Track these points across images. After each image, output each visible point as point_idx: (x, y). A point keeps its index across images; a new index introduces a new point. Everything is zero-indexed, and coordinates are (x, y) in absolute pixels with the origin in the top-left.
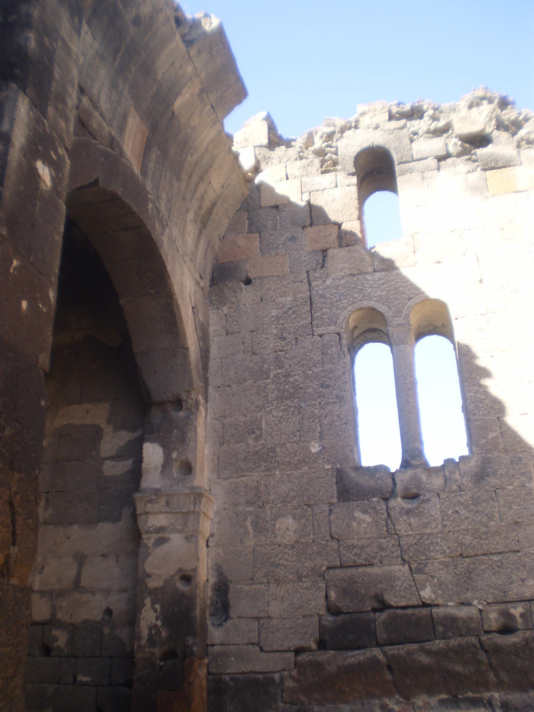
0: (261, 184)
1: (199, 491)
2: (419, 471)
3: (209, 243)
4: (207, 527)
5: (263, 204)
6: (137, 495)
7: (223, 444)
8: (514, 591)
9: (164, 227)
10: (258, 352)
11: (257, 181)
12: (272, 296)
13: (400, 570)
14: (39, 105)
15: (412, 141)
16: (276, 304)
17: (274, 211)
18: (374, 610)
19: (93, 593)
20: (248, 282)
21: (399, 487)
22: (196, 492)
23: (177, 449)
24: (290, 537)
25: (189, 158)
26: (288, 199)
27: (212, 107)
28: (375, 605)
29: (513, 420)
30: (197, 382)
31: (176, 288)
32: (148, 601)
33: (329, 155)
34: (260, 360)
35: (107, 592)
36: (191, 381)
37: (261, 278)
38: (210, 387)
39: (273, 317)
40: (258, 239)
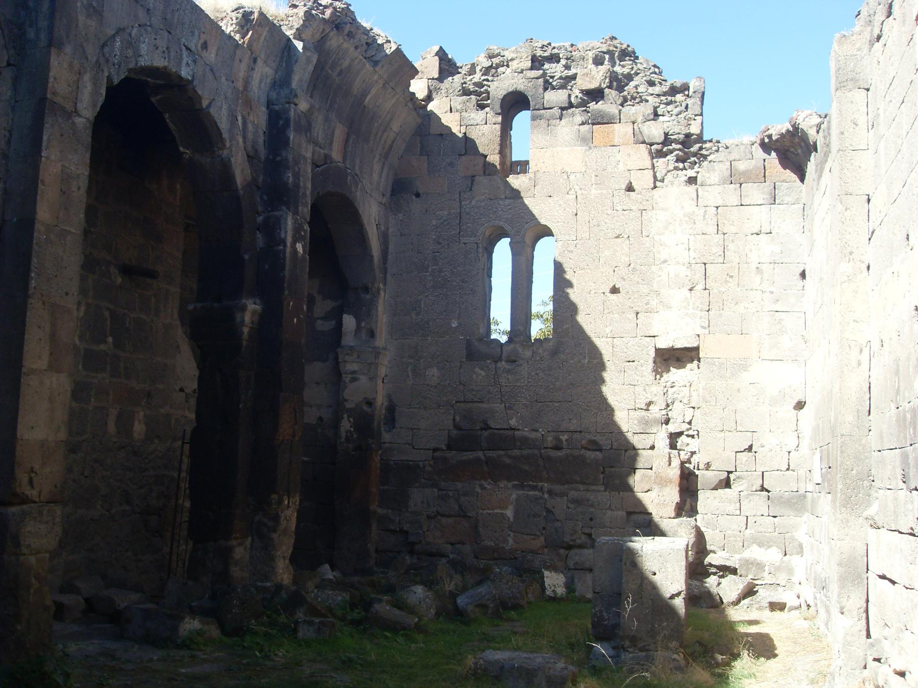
0: (432, 112)
2: (517, 345)
4: (383, 371)
5: (432, 132)
6: (339, 350)
14: (296, 213)
15: (545, 89)
18: (482, 429)
19: (311, 406)
20: (418, 195)
25: (376, 124)
26: (449, 129)
29: (581, 318)
30: (379, 274)
31: (365, 221)
32: (345, 416)
33: (485, 87)
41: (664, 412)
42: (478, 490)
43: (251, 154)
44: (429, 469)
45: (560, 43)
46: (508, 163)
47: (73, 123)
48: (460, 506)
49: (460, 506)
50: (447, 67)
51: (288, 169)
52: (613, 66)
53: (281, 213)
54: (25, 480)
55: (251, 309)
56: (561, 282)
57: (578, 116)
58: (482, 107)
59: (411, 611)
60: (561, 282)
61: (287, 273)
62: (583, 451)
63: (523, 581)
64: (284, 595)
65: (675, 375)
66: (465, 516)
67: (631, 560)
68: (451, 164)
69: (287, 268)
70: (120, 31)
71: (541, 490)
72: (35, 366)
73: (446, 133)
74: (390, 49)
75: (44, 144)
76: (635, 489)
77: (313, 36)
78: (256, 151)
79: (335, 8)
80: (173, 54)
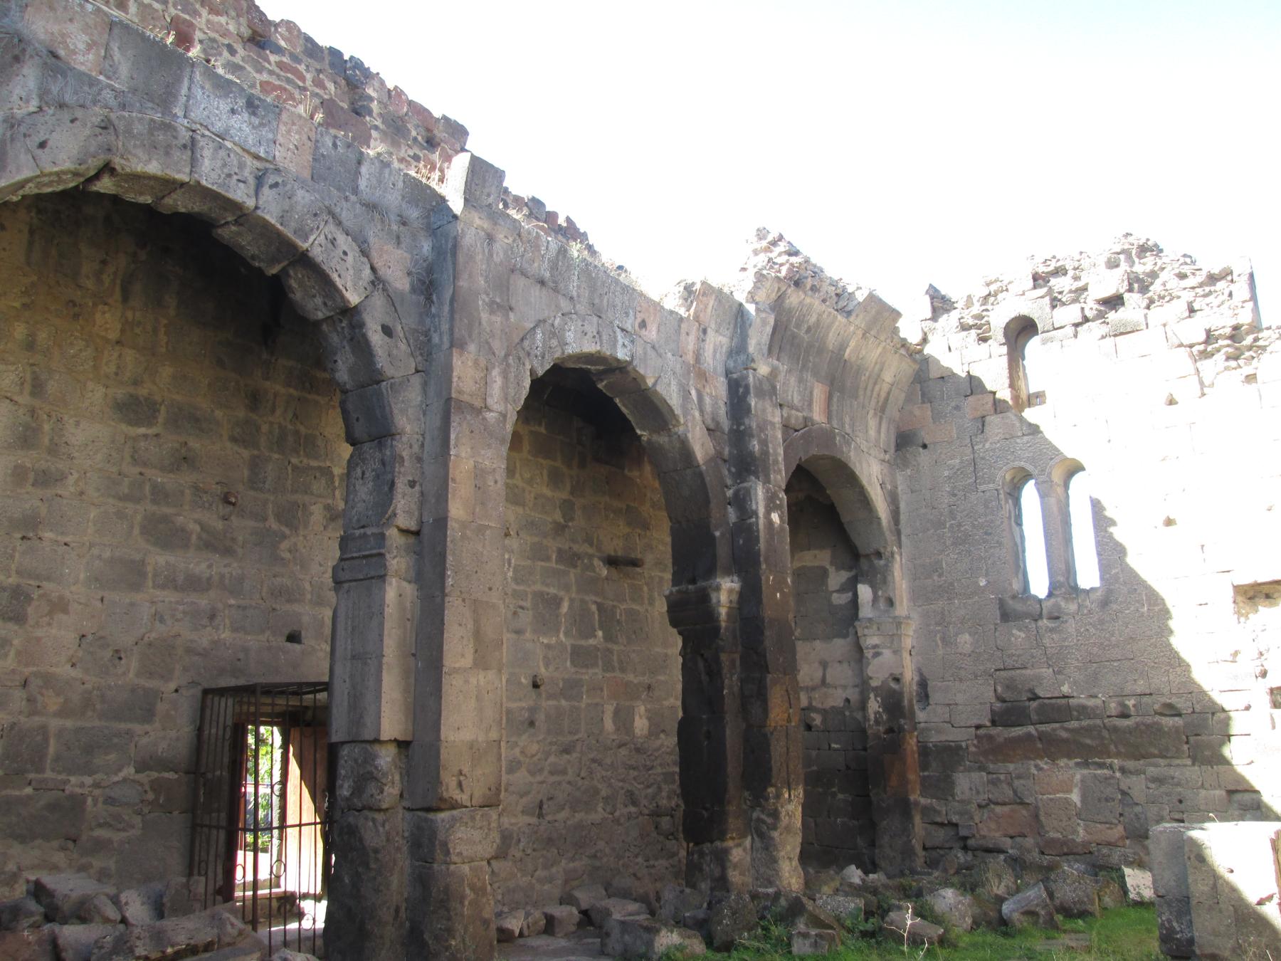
4: (908, 642)
6: (857, 623)
8: (1129, 688)
9: (850, 445)
13: (1047, 672)
14: (767, 481)
15: (1054, 307)
17: (941, 382)
20: (925, 446)
21: (1045, 612)
24: (968, 648)
28: (1030, 695)
29: (1132, 560)
30: (890, 537)
31: (865, 482)
32: (872, 695)
35: (845, 687)
37: (935, 443)
41: (1258, 662)
42: (1034, 771)
43: (712, 427)
44: (972, 749)
45: (1066, 254)
46: (1024, 396)
47: (484, 419)
48: (1015, 792)
49: (1015, 792)
50: (940, 304)
51: (752, 436)
52: (1132, 264)
54: (453, 783)
55: (726, 590)
56: (1101, 521)
57: (1096, 328)
58: (983, 339)
59: (936, 920)
60: (1101, 521)
61: (762, 545)
62: (1157, 718)
63: (1097, 882)
64: (783, 902)
65: (1265, 614)
66: (1022, 803)
67: (1198, 856)
68: (957, 408)
69: (762, 540)
70: (540, 322)
71: (1111, 767)
72: (457, 665)
73: (947, 377)
74: (861, 296)
75: (452, 442)
76: (1234, 762)
77: (768, 296)
78: (718, 423)
79: (792, 264)
80: (605, 337)
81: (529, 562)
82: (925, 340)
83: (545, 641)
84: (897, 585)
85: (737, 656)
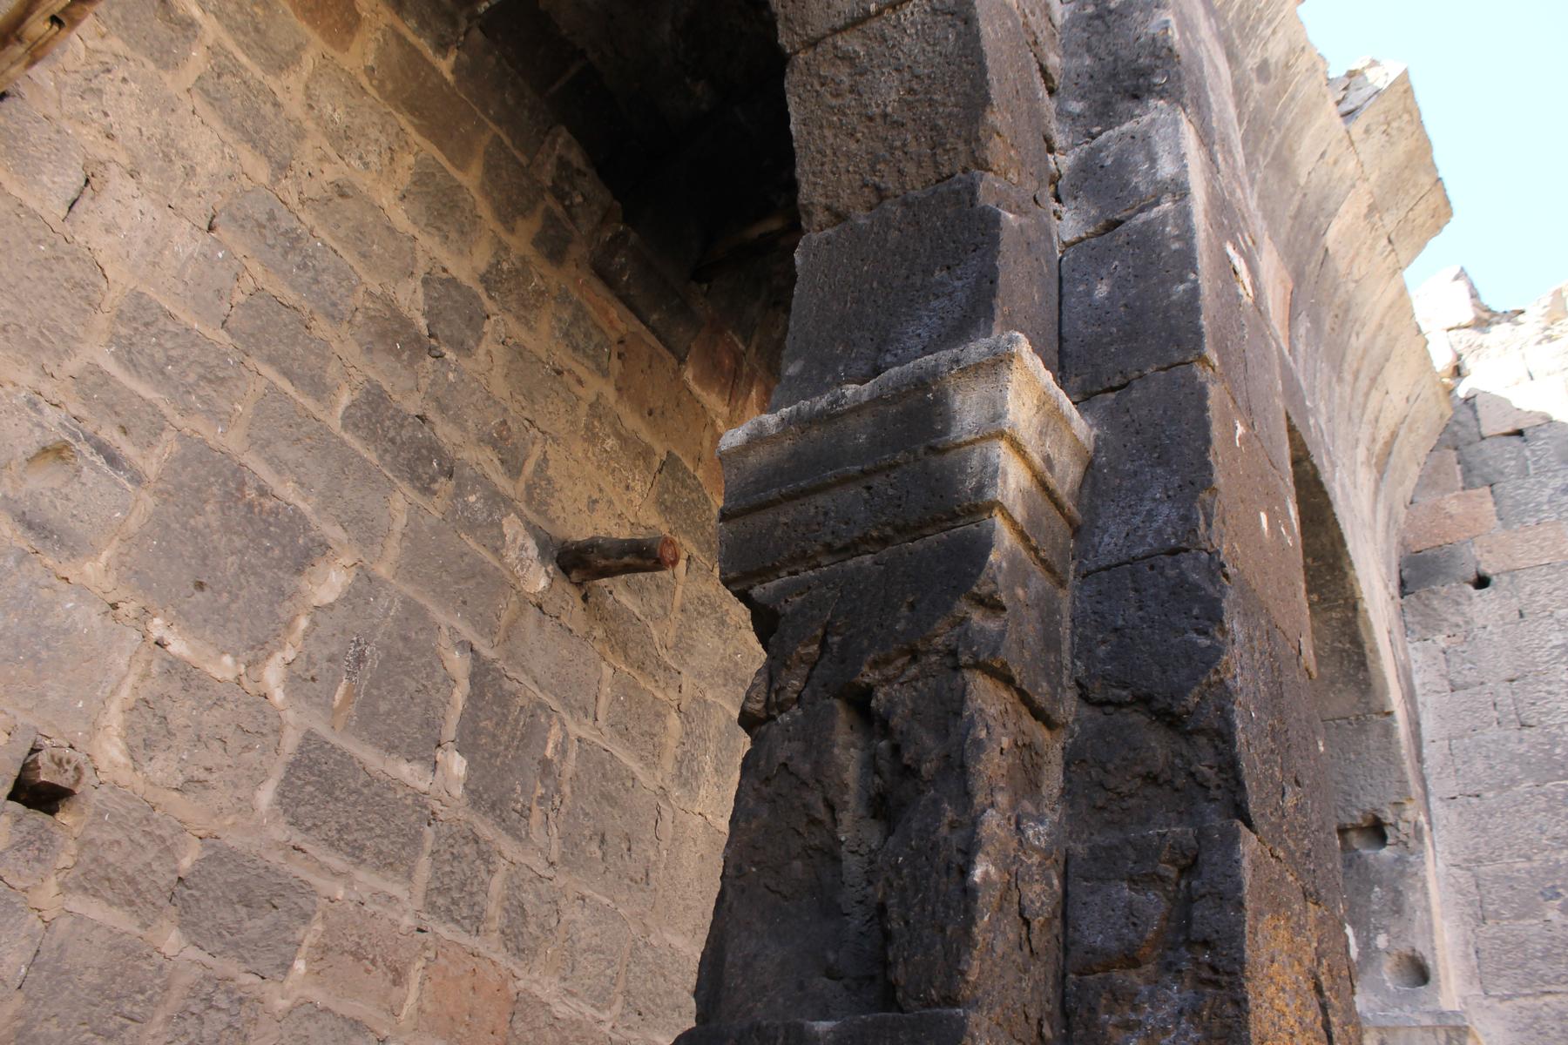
1: (1459, 1022)
3: (1390, 511)
5: (1486, 431)
7: (1484, 919)
10: (1533, 722)
11: (1462, 391)
12: (1544, 607)
16: (1558, 621)
17: (1515, 440)
20: (1482, 582)
22: (1451, 1022)
23: (1387, 932)
25: (1354, 338)
27: (1390, 241)
30: (1415, 788)
34: (1542, 740)
36: (1403, 782)
37: (1512, 572)
38: (1432, 799)
39: (1555, 647)
40: (1490, 498)
53: (1146, 119)
74: (1378, 79)
81: (222, 337)
82: (1457, 372)
83: (177, 646)
84: (1438, 921)
85: (1053, 747)
